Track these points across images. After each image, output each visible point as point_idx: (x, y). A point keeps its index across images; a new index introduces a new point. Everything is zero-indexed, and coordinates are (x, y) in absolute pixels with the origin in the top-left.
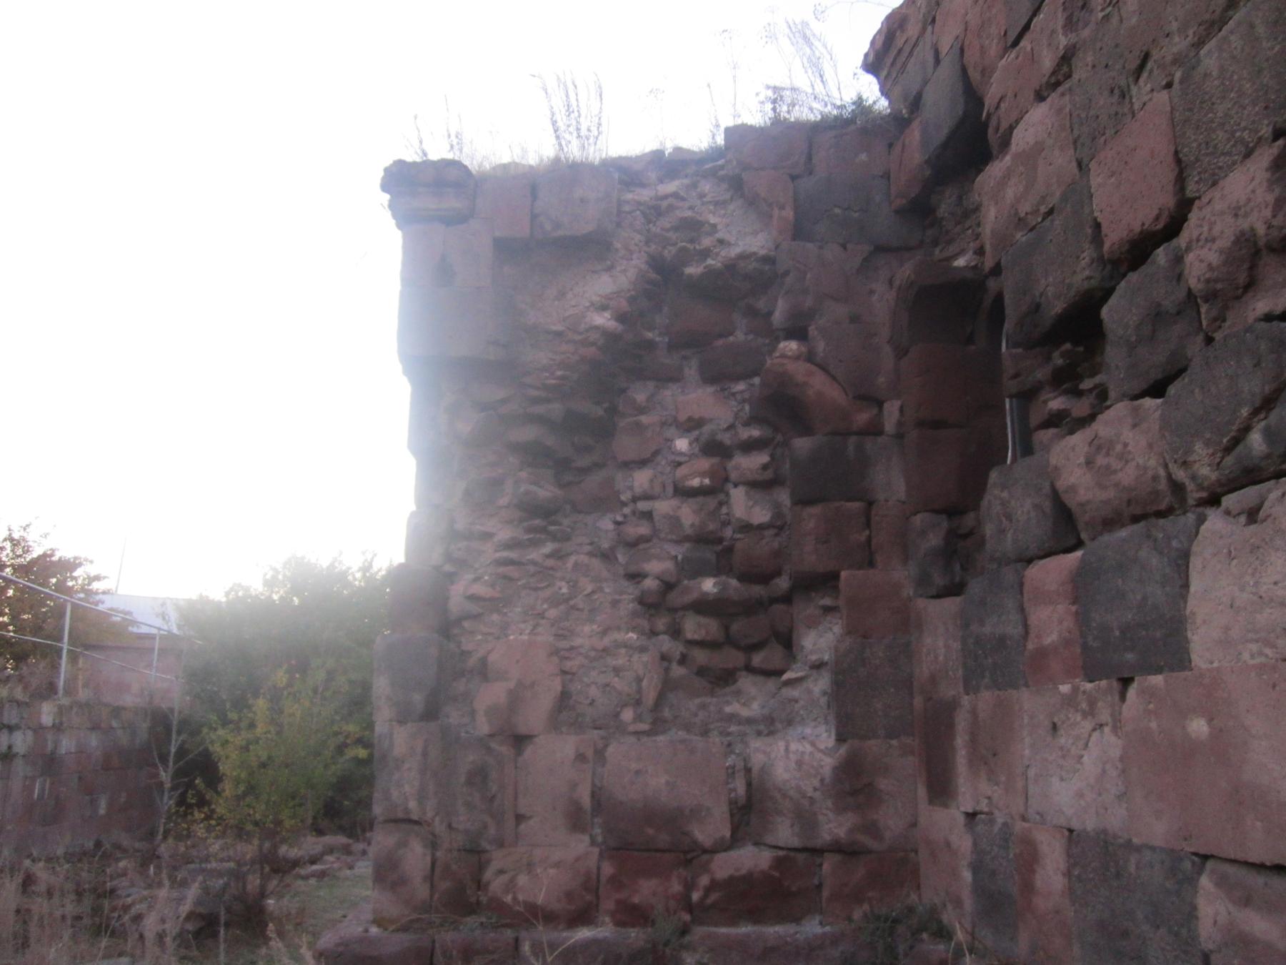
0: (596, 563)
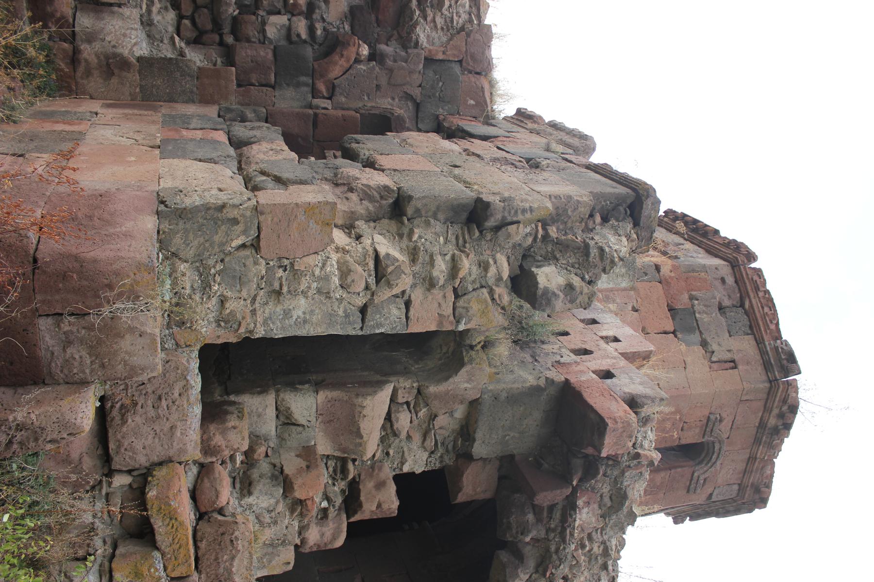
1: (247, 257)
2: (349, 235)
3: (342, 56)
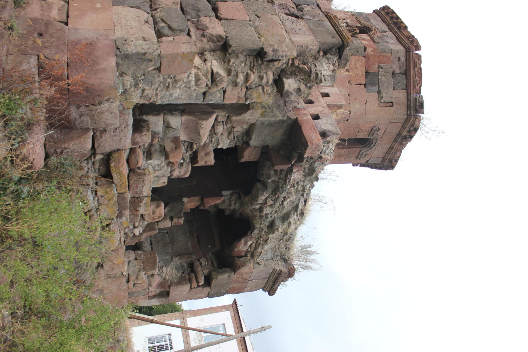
1: (155, 74)
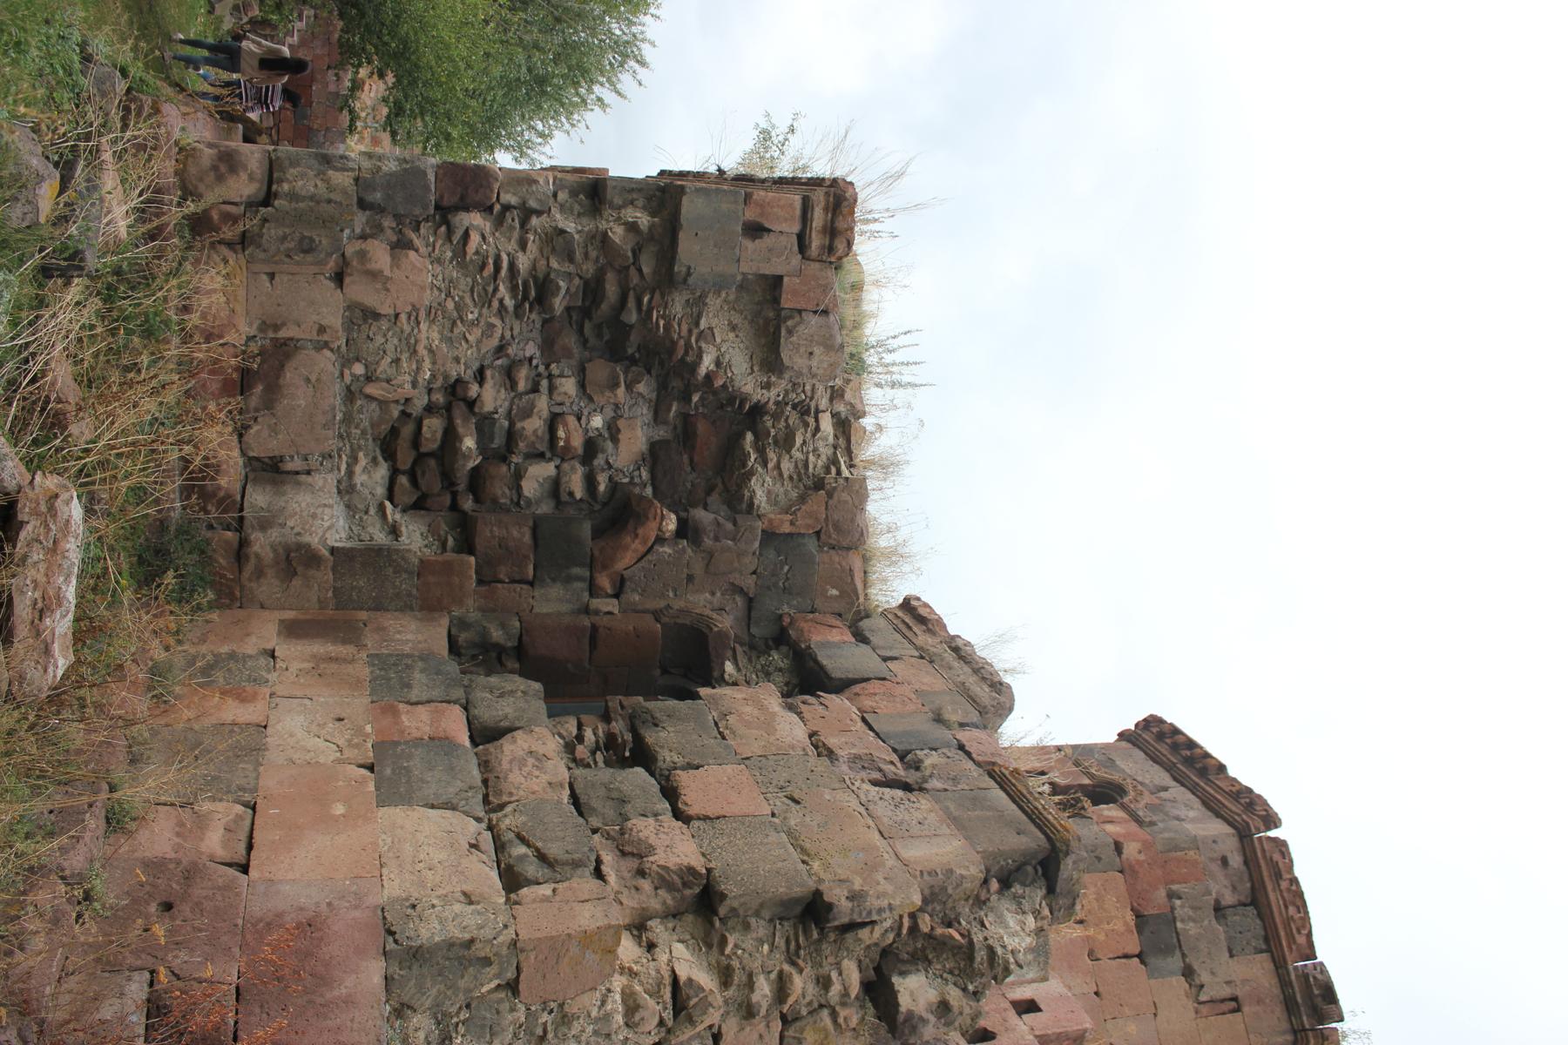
0: (495, 342)
1: (500, 1001)
2: (638, 939)
3: (636, 536)
